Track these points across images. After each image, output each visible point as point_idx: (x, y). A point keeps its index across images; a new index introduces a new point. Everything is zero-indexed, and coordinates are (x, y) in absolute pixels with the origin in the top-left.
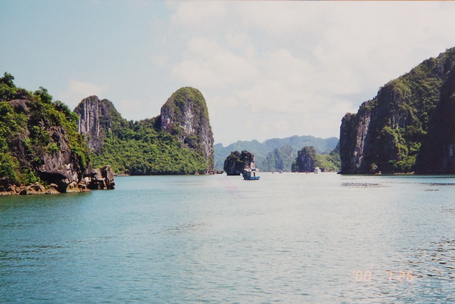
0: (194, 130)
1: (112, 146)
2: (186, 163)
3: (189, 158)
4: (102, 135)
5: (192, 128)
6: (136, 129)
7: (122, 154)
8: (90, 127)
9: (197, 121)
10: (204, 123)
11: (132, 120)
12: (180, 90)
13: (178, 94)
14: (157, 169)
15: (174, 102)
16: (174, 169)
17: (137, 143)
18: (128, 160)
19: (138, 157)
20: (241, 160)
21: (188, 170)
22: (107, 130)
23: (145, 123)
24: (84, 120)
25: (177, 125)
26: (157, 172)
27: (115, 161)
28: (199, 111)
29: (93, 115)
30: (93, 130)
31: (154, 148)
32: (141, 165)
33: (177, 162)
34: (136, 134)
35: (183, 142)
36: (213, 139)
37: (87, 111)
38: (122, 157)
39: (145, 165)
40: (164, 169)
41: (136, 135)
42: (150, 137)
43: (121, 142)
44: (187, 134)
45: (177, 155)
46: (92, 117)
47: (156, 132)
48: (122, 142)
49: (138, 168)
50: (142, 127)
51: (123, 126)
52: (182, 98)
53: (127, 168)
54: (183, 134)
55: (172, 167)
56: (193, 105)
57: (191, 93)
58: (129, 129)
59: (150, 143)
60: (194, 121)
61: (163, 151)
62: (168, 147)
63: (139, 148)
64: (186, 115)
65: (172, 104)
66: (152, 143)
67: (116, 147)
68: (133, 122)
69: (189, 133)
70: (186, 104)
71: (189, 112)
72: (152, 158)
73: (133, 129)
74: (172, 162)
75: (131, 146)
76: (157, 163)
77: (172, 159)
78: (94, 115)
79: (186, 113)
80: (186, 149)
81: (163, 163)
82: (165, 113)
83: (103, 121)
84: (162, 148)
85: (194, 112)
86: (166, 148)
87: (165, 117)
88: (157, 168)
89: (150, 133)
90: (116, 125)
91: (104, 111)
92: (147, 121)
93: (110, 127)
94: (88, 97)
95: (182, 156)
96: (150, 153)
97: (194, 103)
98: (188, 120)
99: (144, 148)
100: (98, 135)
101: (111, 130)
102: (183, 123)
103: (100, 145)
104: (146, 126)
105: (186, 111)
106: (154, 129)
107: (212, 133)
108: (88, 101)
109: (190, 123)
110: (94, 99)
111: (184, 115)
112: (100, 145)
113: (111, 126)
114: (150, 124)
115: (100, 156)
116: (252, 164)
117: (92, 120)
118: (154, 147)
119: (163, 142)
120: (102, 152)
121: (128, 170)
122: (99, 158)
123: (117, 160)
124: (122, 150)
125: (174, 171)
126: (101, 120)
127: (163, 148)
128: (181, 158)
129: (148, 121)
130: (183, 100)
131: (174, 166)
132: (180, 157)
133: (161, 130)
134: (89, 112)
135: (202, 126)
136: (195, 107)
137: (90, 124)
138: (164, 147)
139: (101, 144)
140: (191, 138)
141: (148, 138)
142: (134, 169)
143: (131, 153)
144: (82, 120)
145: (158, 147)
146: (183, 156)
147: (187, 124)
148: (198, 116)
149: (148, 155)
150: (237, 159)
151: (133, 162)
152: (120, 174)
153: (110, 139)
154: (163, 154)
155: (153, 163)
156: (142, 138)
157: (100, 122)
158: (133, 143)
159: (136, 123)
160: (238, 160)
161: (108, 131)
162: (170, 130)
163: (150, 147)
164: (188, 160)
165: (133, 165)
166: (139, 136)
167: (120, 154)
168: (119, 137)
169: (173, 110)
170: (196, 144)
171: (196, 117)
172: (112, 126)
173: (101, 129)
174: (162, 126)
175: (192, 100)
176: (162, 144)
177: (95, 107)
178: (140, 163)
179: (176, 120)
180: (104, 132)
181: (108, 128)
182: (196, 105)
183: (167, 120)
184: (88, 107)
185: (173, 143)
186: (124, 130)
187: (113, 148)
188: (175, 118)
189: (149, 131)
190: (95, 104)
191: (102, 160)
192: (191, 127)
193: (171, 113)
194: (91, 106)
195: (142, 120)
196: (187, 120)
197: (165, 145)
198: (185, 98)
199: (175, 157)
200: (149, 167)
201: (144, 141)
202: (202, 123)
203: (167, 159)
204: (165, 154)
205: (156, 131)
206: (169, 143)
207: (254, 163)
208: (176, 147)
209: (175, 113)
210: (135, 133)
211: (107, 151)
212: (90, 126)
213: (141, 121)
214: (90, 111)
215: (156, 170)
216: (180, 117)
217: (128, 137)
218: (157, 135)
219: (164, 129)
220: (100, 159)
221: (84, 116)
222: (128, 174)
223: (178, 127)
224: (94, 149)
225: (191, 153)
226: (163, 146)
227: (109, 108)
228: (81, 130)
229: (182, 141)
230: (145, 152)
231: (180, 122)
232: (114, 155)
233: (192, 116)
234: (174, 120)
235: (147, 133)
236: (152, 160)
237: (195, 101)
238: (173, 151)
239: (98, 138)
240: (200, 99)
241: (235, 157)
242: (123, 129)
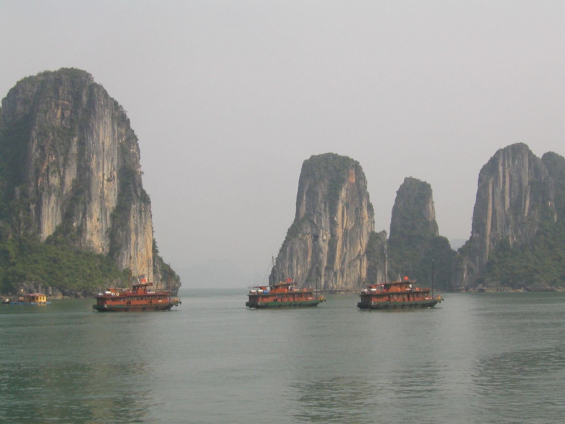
30: (517, 206)
37: (504, 172)
194: (513, 162)
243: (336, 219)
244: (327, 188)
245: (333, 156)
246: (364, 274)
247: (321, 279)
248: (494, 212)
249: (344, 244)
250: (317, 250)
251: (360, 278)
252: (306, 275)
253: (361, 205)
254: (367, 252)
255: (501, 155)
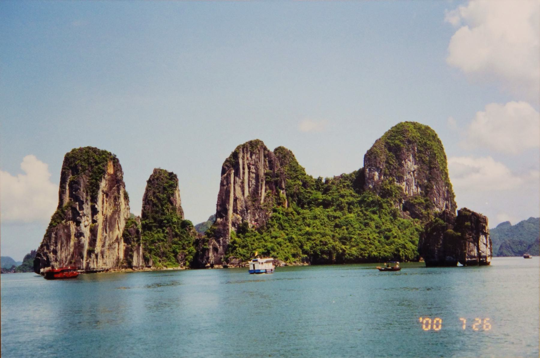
0: (419, 190)
1: (286, 218)
2: (403, 242)
3: (412, 234)
4: (269, 200)
5: (417, 186)
6: (326, 191)
7: (300, 230)
8: (250, 190)
9: (424, 175)
10: (436, 178)
11: (319, 177)
12: (396, 127)
13: (392, 132)
14: (354, 253)
15: (385, 146)
16: (382, 252)
17: (326, 213)
18: (308, 239)
19: (324, 235)
20: (455, 229)
21: (407, 254)
22: (277, 193)
23: (339, 181)
24: (240, 178)
25: (390, 183)
26: (354, 258)
27: (287, 241)
28: (428, 158)
29: (254, 171)
30: (255, 194)
31: (352, 219)
32: (328, 248)
33: (387, 242)
34: (324, 198)
35: (402, 210)
36: (455, 203)
37: (244, 165)
38: (300, 235)
39: (334, 248)
40: (365, 253)
41: (324, 200)
42: (347, 203)
43: (300, 211)
44: (408, 196)
45: (390, 230)
46: (253, 173)
47: (357, 195)
48: (302, 211)
49: (323, 252)
50: (334, 187)
51: (305, 188)
52: (398, 139)
53: (305, 252)
54: (401, 196)
55: (379, 250)
56: (417, 149)
57: (415, 130)
58: (315, 191)
59: (346, 212)
60: (418, 174)
61: (366, 225)
62: (376, 217)
63: (327, 220)
64: (405, 166)
65: (382, 149)
66: (350, 212)
67: (292, 219)
68: (321, 180)
69: (412, 195)
70: (406, 148)
71: (410, 161)
72: (347, 235)
73: (321, 191)
74: (379, 242)
75: (315, 218)
76: (353, 244)
77: (381, 237)
78: (256, 170)
79: (406, 162)
80: (405, 220)
81: (365, 243)
82: (370, 163)
83: (271, 180)
84: (365, 220)
85: (419, 160)
86: (372, 220)
87: (370, 170)
88: (354, 251)
89: (347, 196)
90: (295, 185)
91: (273, 164)
92: (344, 177)
93: (283, 189)
94: (246, 143)
95: (399, 231)
96: (345, 227)
97: (419, 147)
98: (409, 173)
99: (337, 219)
100: (262, 202)
101: (285, 193)
102: (400, 179)
103: (265, 218)
104: (341, 185)
105: (405, 160)
106: (354, 189)
107: (453, 194)
108: (245, 149)
109: (413, 178)
110: (256, 145)
111: (401, 165)
112: (265, 218)
113: (284, 187)
114: (348, 182)
115: (265, 234)
116: (482, 238)
117: (252, 178)
118: (351, 217)
119: (367, 210)
120: (268, 228)
121: (306, 256)
122: (263, 238)
123: (291, 240)
124: (302, 224)
125: (382, 257)
126: (269, 178)
127: (367, 219)
128: (395, 234)
129: (345, 178)
130: (400, 141)
131: (383, 248)
132: (394, 233)
133: (364, 190)
134: (248, 165)
135: (433, 183)
136: (420, 153)
137: (250, 184)
138: (368, 217)
139: (267, 216)
140: (415, 202)
141: (343, 204)
142: (315, 255)
143: (314, 229)
144: (236, 177)
145: (360, 218)
146: (401, 232)
147: (407, 181)
148: (425, 167)
149: (341, 231)
150: (447, 229)
151: (315, 243)
152: (294, 264)
153: (283, 207)
154: (365, 228)
155: (348, 243)
156: (334, 204)
157: (266, 181)
158: (319, 213)
159: (327, 181)
160: (450, 231)
161: (278, 195)
162: (378, 191)
163: (345, 218)
164: (408, 238)
165: (314, 248)
166: (328, 201)
167: (298, 230)
168: (298, 204)
169: (384, 158)
170: (423, 211)
171: (422, 168)
172: (286, 187)
173: (269, 191)
174: (366, 185)
175: (416, 141)
176: (365, 212)
177: (257, 158)
178: (325, 244)
179: (388, 173)
180: (272, 196)
181: (279, 190)
182: (422, 149)
183: (374, 175)
184: (245, 157)
185: (384, 211)
186: (308, 192)
187: (287, 221)
188: (387, 171)
189: (346, 192)
190: (258, 152)
191: (265, 241)
192: (414, 184)
193: (380, 163)
194: (251, 156)
195: (336, 176)
196: (407, 174)
197: (371, 214)
198: (403, 139)
199: (386, 233)
200: (341, 251)
201: (338, 209)
202: (433, 178)
203: (371, 237)
204: (369, 228)
205: (357, 192)
206: (378, 212)
207: (488, 236)
208: (388, 218)
209: (387, 162)
210: (324, 197)
211: (276, 226)
212: (249, 187)
213: (335, 178)
214: (249, 163)
215: (352, 255)
216: (395, 168)
217: (312, 204)
218: (359, 199)
219: (369, 188)
220: (264, 240)
221: (240, 172)
222: (307, 262)
223: (391, 186)
224: (255, 223)
225: (416, 226)
226: (368, 215)
227: (285, 159)
228: (234, 194)
229: (399, 207)
230: (336, 226)
231: (396, 177)
232: (287, 232)
233: (416, 167)
234: (385, 175)
235: (343, 196)
236: (346, 238)
237: (420, 142)
238: (383, 223)
239: (262, 206)
240: (429, 140)
241: (441, 224)
242: (305, 191)
243: (96, 206)
244: (367, 200)
245: (92, 150)
246: (122, 256)
247: (83, 260)
248: (236, 199)
249: (105, 229)
250: (80, 235)
251: (118, 259)
252: (69, 257)
253: (119, 193)
254: (124, 235)
255: (241, 149)
